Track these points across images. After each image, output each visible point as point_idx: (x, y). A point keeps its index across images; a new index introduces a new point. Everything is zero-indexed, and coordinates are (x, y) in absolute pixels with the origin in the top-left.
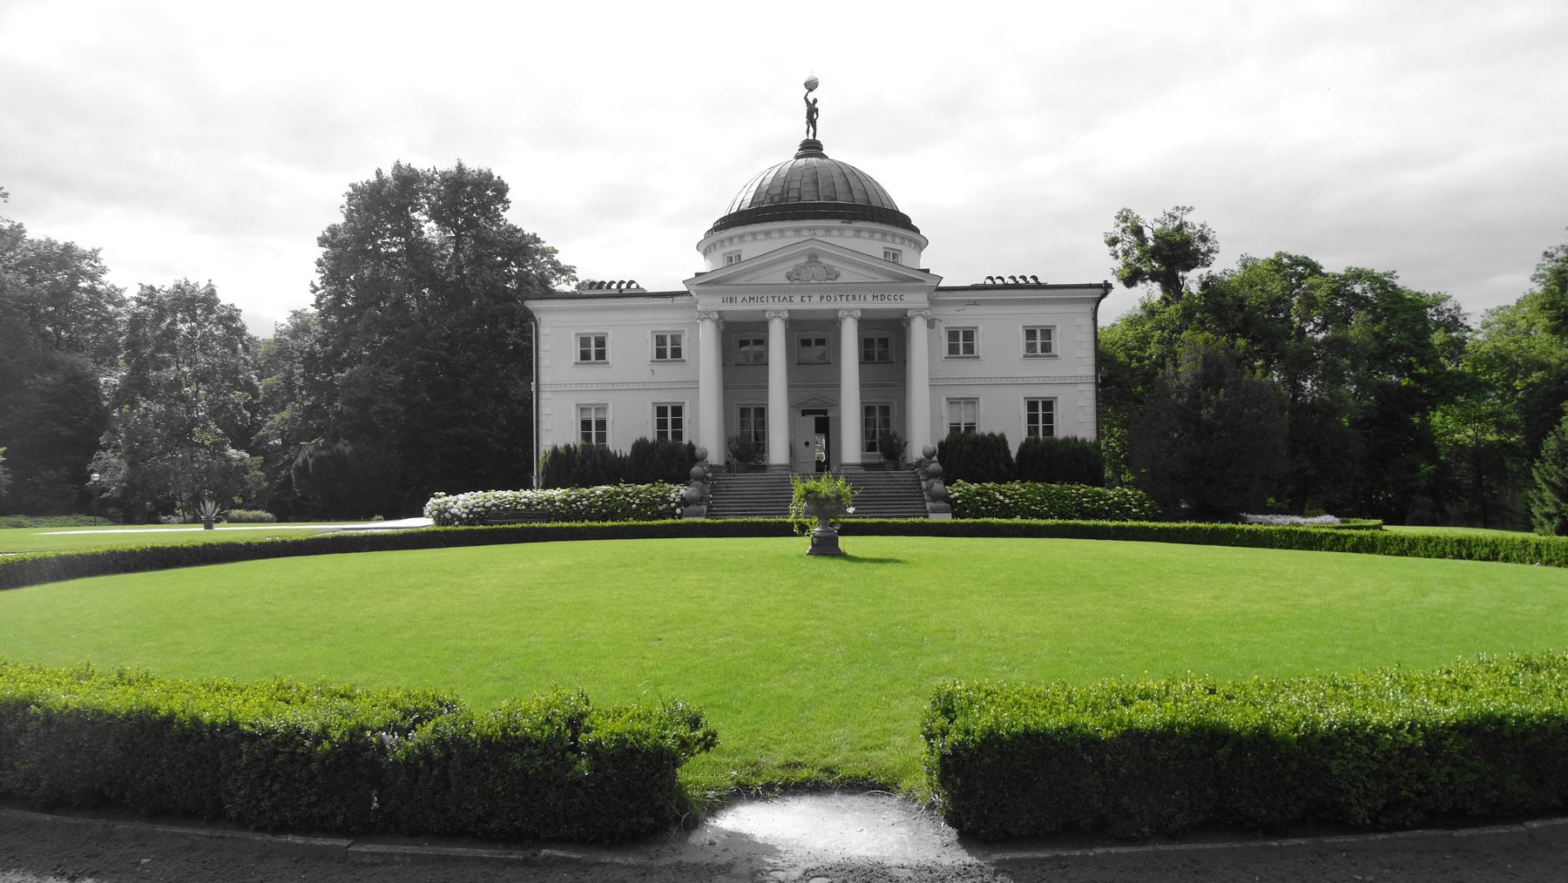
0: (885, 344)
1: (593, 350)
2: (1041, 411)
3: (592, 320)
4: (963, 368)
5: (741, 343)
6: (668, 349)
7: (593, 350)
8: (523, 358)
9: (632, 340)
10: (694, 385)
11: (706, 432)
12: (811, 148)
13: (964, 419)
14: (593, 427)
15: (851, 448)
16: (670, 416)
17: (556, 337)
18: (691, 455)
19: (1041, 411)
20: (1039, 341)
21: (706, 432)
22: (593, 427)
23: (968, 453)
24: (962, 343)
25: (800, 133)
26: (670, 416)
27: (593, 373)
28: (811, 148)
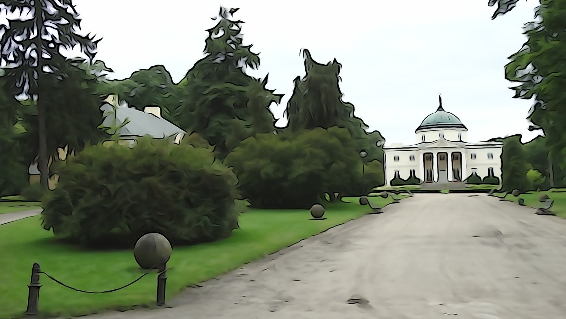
0: (457, 157)
1: (396, 159)
2: (491, 171)
3: (396, 154)
4: (474, 161)
5: (428, 157)
6: (412, 158)
7: (396, 159)
8: (382, 160)
9: (404, 156)
10: (418, 166)
11: (420, 175)
12: (440, 108)
13: (474, 171)
14: (397, 175)
15: (451, 178)
16: (412, 173)
17: (389, 157)
18: (419, 180)
19: (491, 171)
20: (491, 156)
21: (420, 175)
22: (397, 175)
23: (474, 179)
24: (473, 156)
25: (439, 106)
26: (412, 173)
27: (397, 163)
28: (440, 108)
